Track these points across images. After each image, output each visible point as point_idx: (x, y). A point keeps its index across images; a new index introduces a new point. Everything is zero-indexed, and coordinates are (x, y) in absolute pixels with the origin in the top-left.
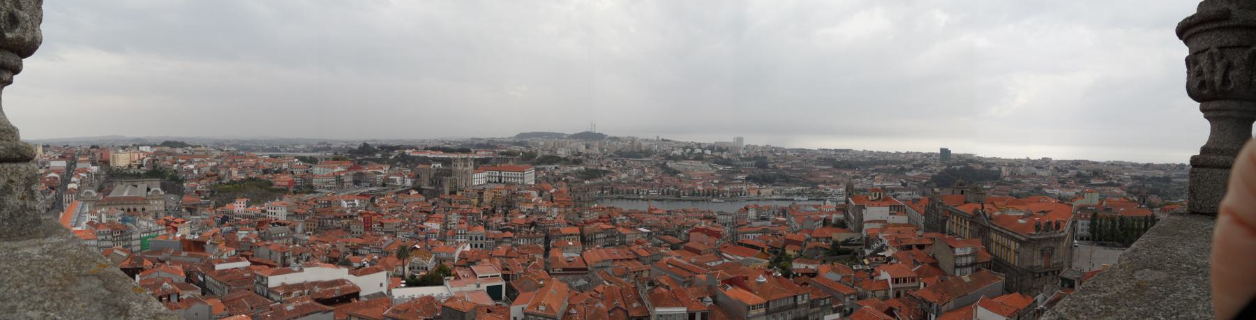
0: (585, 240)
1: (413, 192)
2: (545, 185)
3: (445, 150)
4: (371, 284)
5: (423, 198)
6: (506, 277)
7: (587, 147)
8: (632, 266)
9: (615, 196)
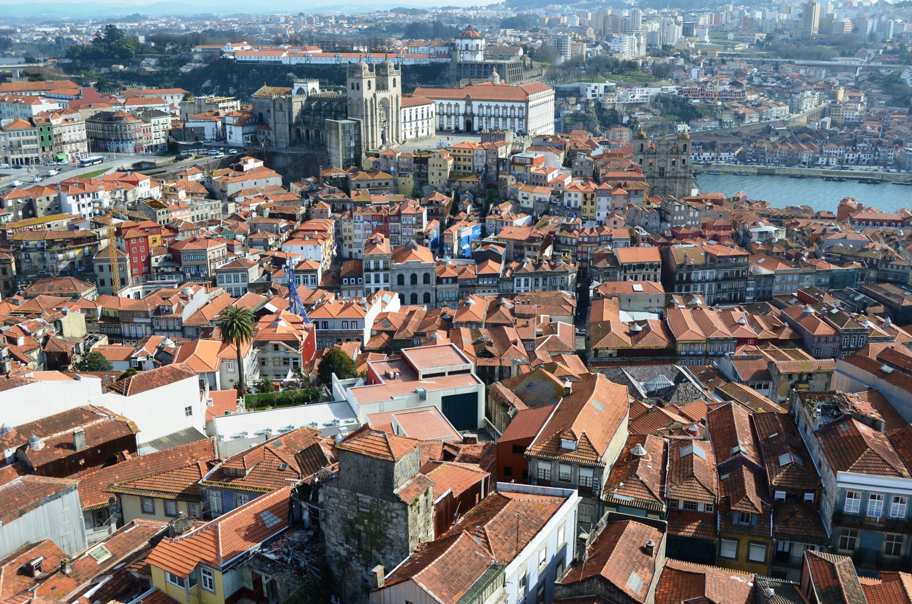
0: (673, 278)
1: (251, 164)
2: (581, 138)
3: (328, 45)
4: (159, 413)
5: (276, 180)
6: (486, 374)
7: (687, 32)
8: (793, 362)
9: (753, 168)
